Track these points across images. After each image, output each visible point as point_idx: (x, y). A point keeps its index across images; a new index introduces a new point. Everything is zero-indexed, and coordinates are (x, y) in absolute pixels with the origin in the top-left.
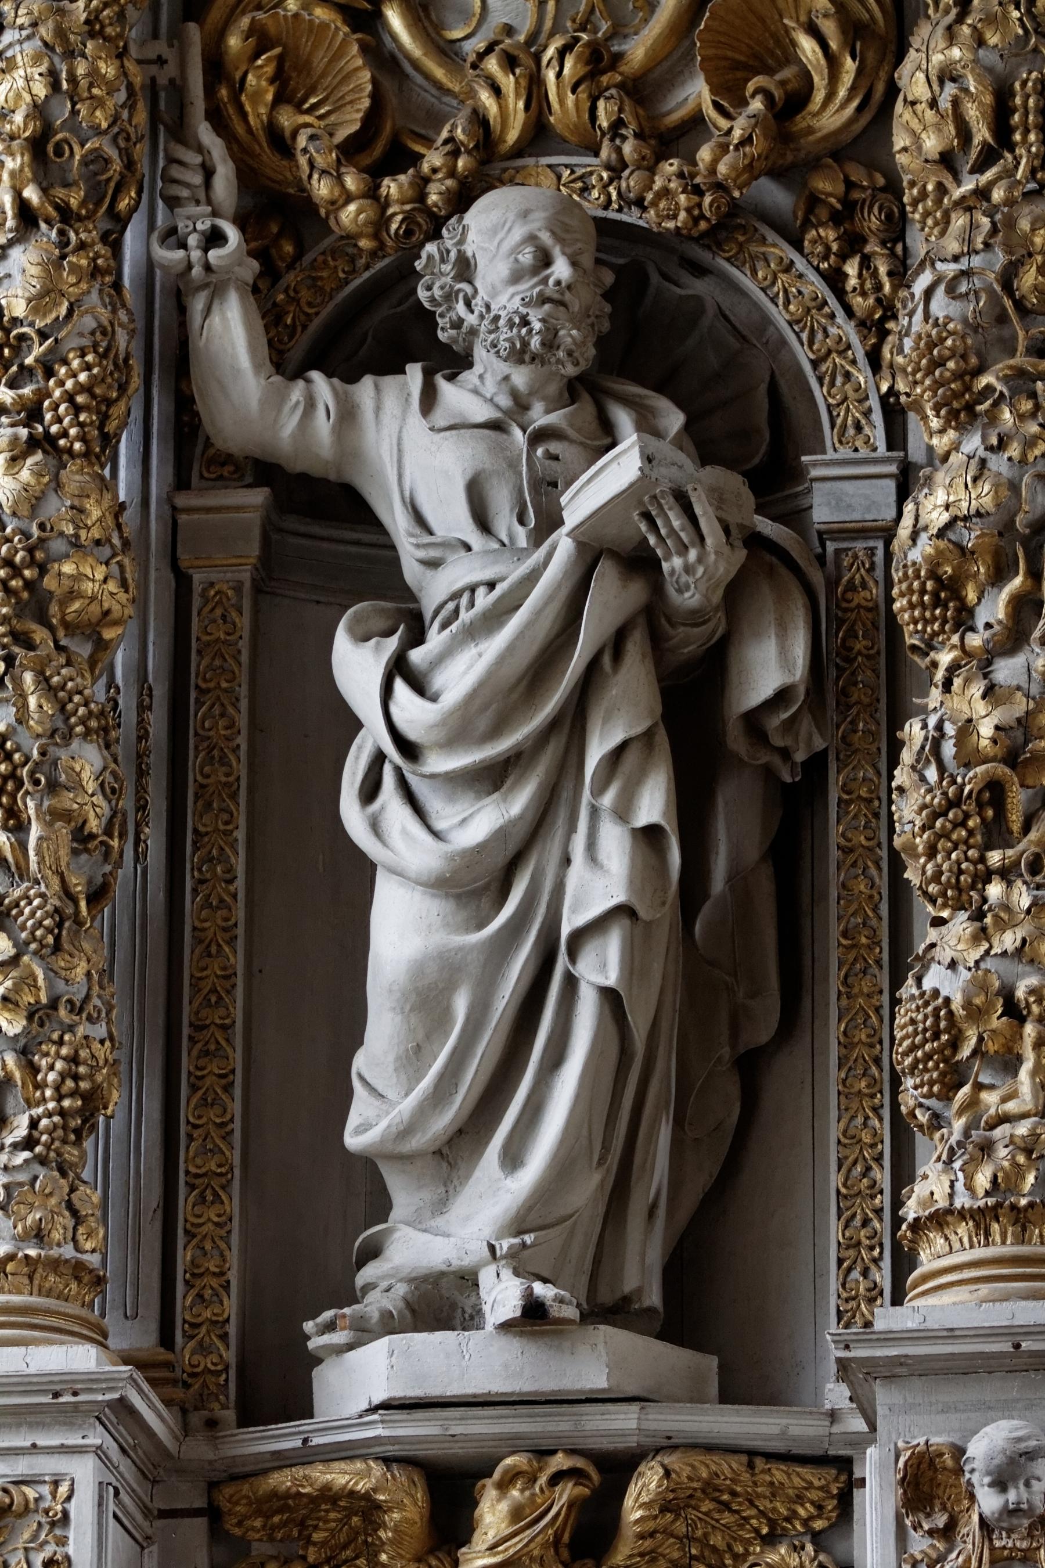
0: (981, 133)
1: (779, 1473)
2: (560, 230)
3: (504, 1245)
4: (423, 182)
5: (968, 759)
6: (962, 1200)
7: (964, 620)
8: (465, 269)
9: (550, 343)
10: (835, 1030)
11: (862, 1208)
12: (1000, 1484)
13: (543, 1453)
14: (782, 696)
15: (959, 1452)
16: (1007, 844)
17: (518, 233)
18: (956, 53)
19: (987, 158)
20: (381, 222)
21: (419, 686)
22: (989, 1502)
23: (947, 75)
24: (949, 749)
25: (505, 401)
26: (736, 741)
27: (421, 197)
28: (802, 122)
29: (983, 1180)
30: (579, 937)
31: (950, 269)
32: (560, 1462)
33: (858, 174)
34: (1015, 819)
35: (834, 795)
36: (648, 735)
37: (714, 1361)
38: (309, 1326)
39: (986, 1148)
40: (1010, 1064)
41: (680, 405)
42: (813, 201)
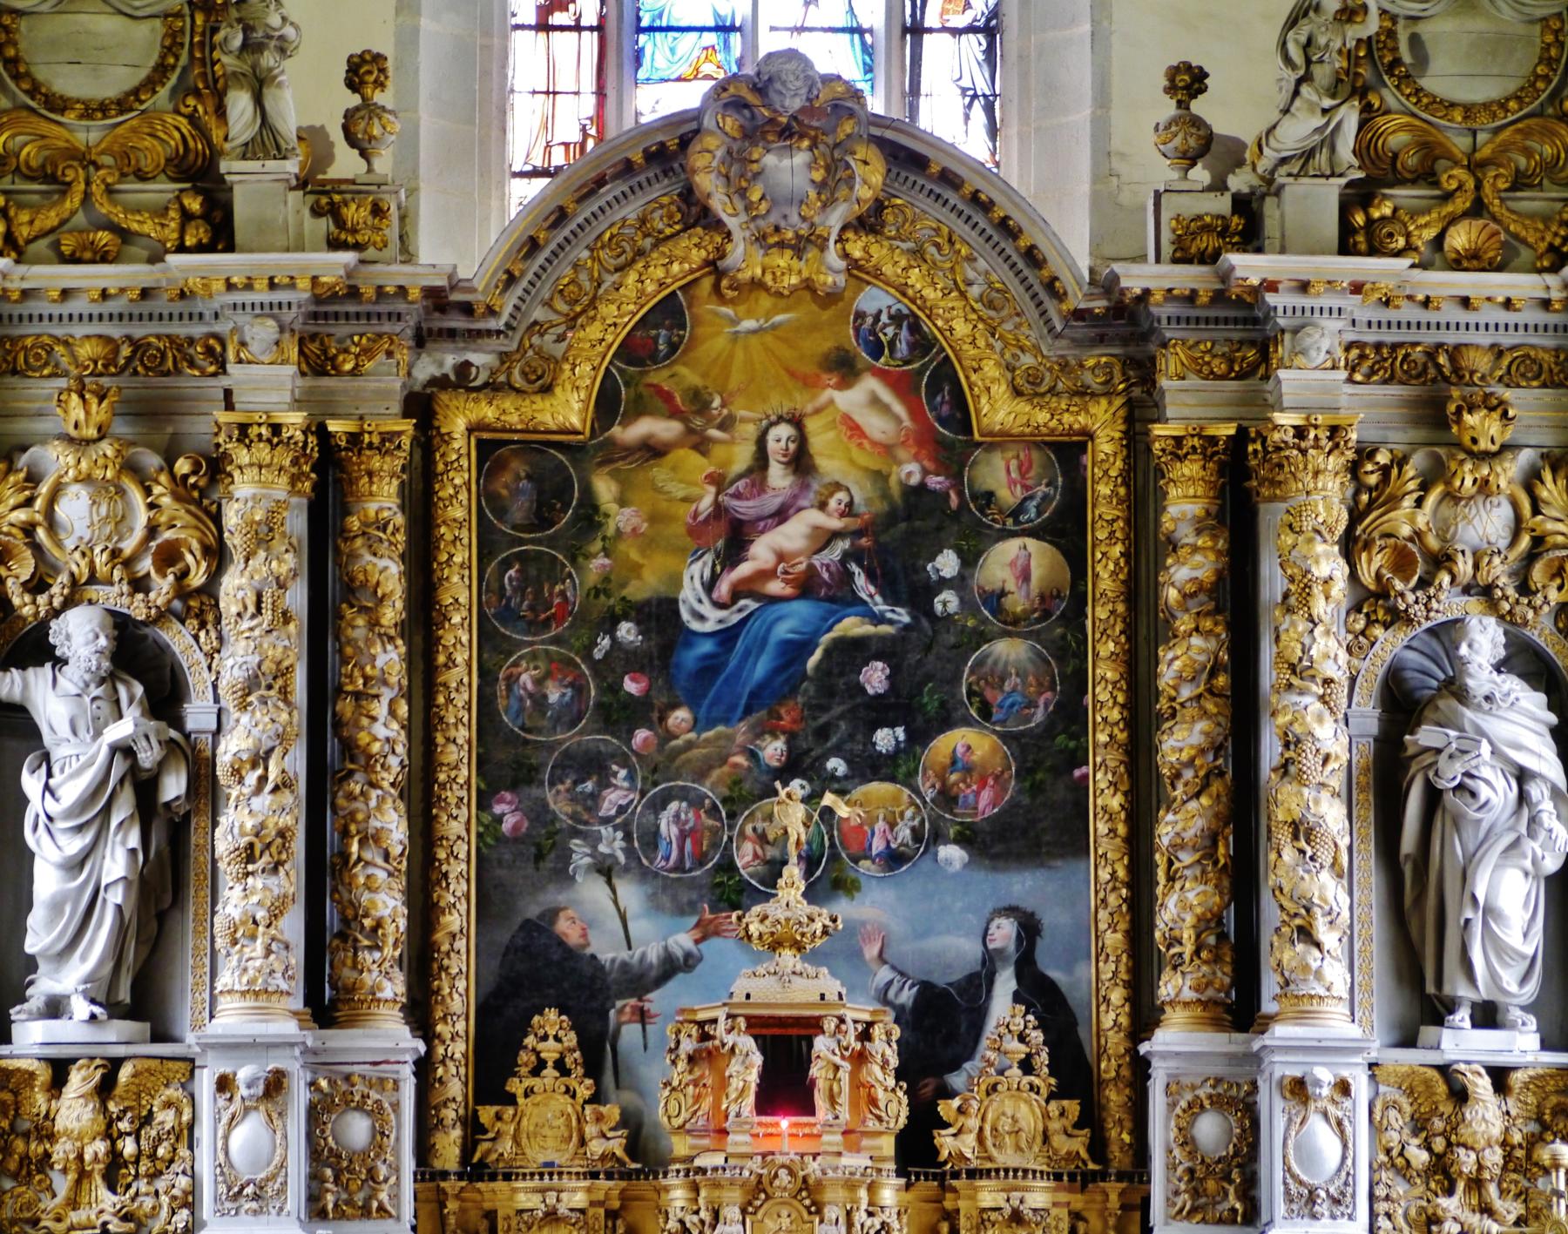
0: (251, 609)
1: (170, 1064)
2: (103, 627)
3: (81, 988)
4: (52, 597)
5: (243, 834)
6: (237, 987)
7: (241, 781)
8: (68, 637)
9: (98, 668)
10: (192, 909)
11: (199, 972)
12: (249, 1086)
13: (92, 1058)
14: (178, 798)
15: (235, 1074)
16: (254, 862)
17: (88, 628)
18: (244, 580)
19: (253, 617)
20: (37, 613)
21: (53, 794)
22: (244, 1091)
23: (240, 588)
24: (236, 831)
25: (82, 685)
26: (161, 810)
27: (51, 603)
28: (186, 581)
29: (245, 980)
30: (107, 886)
31: (240, 660)
32: (98, 1062)
33: (205, 599)
34: (257, 853)
35: (193, 826)
36: (132, 815)
37: (147, 1026)
38: (12, 1011)
39: (245, 970)
40: (253, 938)
41: (142, 682)
42: (189, 608)
